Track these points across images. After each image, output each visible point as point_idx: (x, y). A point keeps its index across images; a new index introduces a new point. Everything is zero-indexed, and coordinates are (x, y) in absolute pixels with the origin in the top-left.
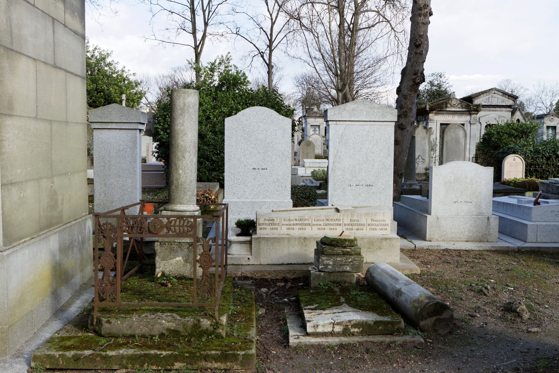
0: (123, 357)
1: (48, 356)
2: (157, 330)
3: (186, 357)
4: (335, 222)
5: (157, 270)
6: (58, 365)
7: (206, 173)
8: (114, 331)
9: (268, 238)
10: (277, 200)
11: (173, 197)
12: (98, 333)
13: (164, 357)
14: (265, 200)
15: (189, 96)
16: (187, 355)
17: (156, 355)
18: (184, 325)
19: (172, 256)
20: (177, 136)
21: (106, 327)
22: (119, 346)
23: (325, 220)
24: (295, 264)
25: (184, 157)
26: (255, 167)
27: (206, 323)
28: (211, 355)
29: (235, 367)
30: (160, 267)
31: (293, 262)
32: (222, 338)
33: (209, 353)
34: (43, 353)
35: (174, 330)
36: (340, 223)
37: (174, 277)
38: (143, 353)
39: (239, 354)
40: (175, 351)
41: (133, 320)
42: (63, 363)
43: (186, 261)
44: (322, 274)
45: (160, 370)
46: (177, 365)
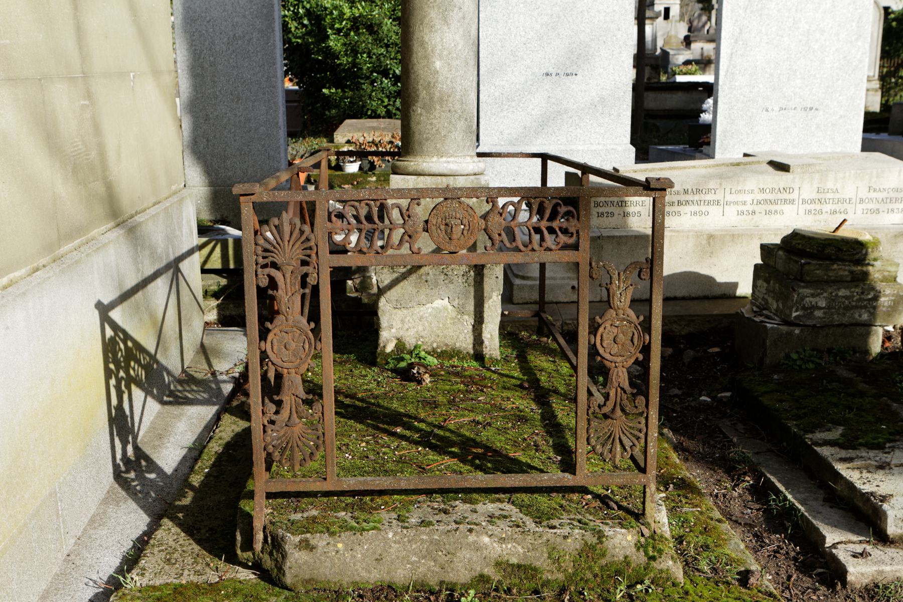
4: (780, 196)
7: (383, 102)
9: (621, 237)
10: (601, 147)
11: (417, 137)
14: (573, 147)
19: (422, 297)
21: (298, 562)
23: (756, 190)
24: (683, 298)
25: (445, 21)
26: (551, 70)
27: (622, 541)
30: (391, 327)
31: (679, 294)
35: (519, 566)
36: (791, 197)
37: (429, 353)
41: (386, 539)
43: (461, 311)
44: (797, 331)
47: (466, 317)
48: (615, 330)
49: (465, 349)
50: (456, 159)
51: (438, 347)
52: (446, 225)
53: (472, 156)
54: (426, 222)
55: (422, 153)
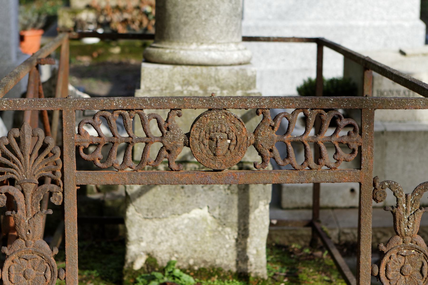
9: (408, 132)
10: (384, 23)
11: (173, 20)
19: (178, 206)
30: (140, 240)
37: (184, 271)
43: (222, 221)
47: (228, 230)
48: (402, 260)
49: (226, 266)
50: (219, 47)
51: (195, 264)
52: (211, 139)
53: (237, 43)
54: (188, 135)
55: (178, 39)
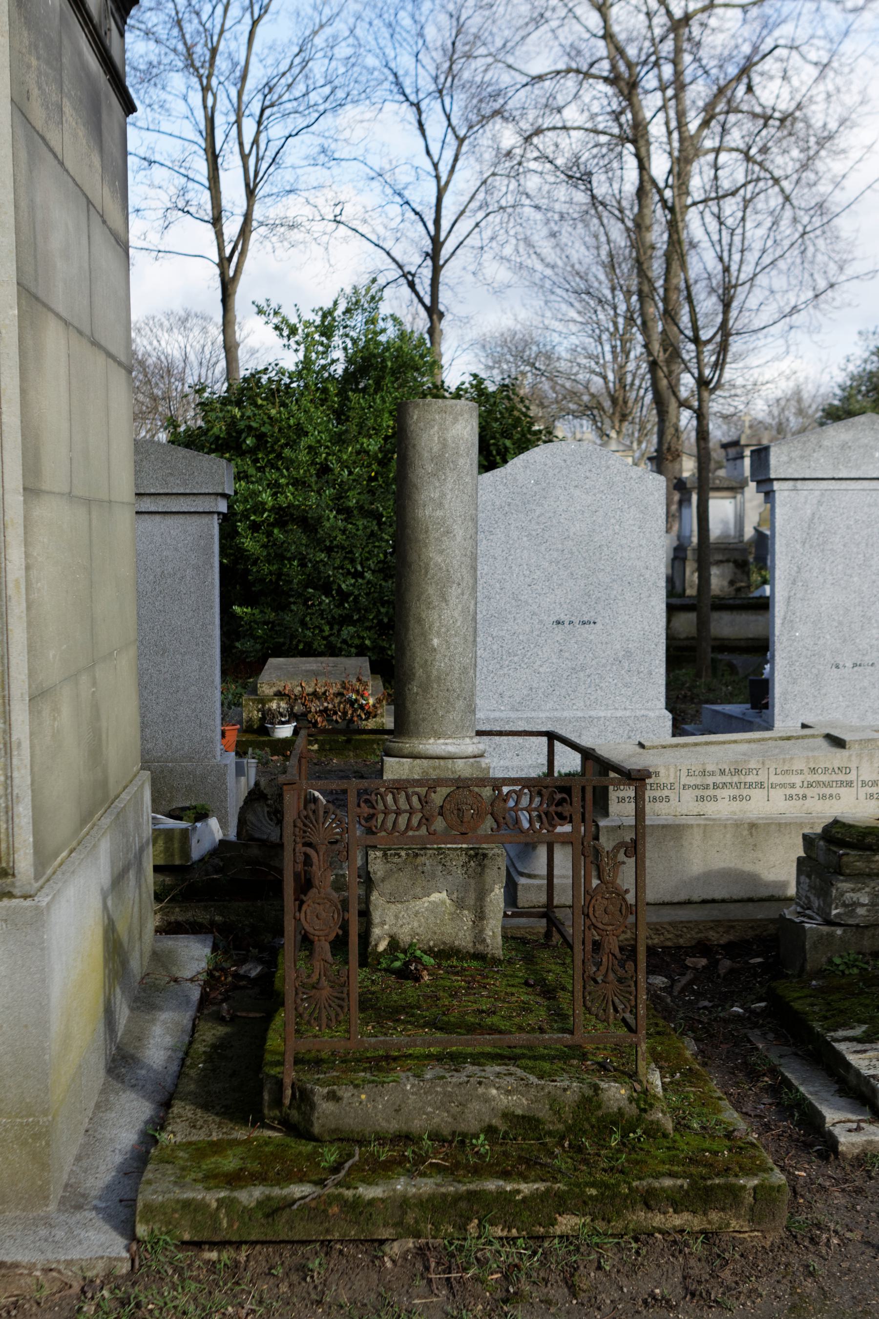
0: (404, 1203)
1: (187, 1204)
2: (475, 1116)
3: (591, 1197)
4: (834, 777)
5: (376, 931)
6: (216, 1229)
7: (322, 631)
8: (351, 1122)
10: (628, 713)
11: (412, 717)
12: (300, 1130)
13: (524, 1200)
14: (593, 713)
15: (456, 420)
16: (593, 1192)
17: (501, 1193)
18: (553, 1101)
20: (422, 536)
21: (326, 1113)
22: (379, 1170)
23: (806, 770)
24: (723, 901)
25: (444, 598)
26: (562, 617)
27: (616, 1094)
28: (663, 1189)
29: (733, 1223)
30: (383, 923)
31: (718, 896)
32: (665, 1136)
33: (657, 1185)
34: (171, 1196)
35: (523, 1117)
36: (848, 778)
37: (425, 952)
38: (463, 1188)
39: (743, 1187)
40: (555, 1180)
41: (404, 1091)
42: (230, 1225)
43: (460, 904)
44: (839, 932)
45: (514, 1239)
46: (566, 1223)
47: (466, 912)
48: (606, 902)
49: (465, 947)
50: (454, 741)
51: (435, 946)
52: (459, 809)
53: (471, 738)
54: (442, 807)
55: (417, 734)
